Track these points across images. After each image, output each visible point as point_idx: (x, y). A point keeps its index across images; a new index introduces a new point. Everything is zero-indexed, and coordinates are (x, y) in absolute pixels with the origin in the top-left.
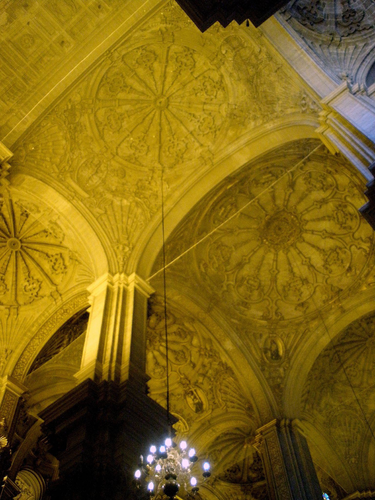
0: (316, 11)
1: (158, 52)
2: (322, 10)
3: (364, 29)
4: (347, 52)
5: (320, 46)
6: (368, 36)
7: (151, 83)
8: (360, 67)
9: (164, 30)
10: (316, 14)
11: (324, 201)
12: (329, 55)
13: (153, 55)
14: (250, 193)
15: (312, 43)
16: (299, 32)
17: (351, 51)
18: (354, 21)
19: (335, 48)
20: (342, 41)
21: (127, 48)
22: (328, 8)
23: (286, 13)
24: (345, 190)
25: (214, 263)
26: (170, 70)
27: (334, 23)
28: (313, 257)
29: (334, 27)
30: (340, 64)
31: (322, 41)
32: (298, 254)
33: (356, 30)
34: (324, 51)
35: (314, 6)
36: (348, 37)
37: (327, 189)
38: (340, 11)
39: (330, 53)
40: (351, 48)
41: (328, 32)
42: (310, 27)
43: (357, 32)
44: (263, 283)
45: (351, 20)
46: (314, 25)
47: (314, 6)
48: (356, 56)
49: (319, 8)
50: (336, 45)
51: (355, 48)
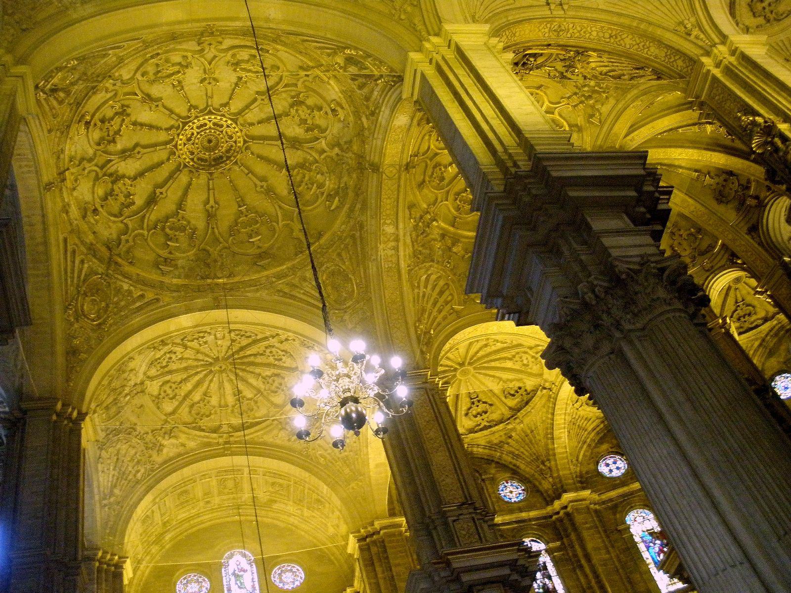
1: (187, 409)
7: (214, 386)
9: (167, 437)
11: (125, 154)
13: (193, 412)
14: (209, 223)
21: (207, 437)
24: (89, 172)
25: (321, 186)
26: (189, 386)
28: (196, 81)
32: (212, 97)
37: (111, 175)
44: (290, 100)
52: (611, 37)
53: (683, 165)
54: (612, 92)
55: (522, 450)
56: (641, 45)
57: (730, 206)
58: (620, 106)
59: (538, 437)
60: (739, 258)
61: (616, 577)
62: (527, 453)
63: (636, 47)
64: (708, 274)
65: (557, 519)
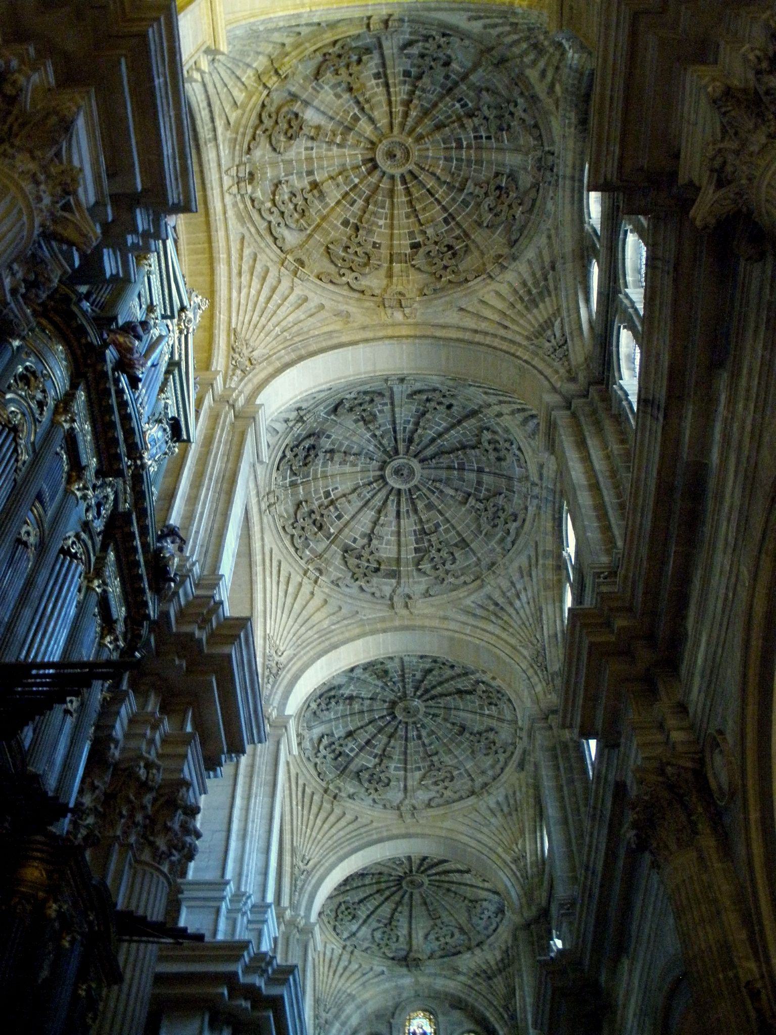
0: (339, 78)
2: (333, 87)
3: (254, 138)
4: (239, 84)
5: (283, 45)
6: (239, 137)
8: (206, 91)
10: (337, 73)
12: (259, 50)
15: (299, 34)
16: (332, 25)
17: (236, 93)
18: (277, 128)
19: (260, 70)
20: (261, 88)
22: (328, 99)
23: (382, 26)
27: (298, 93)
29: (293, 89)
30: (234, 59)
31: (287, 55)
33: (261, 122)
34: (271, 46)
35: (349, 79)
36: (260, 102)
38: (310, 116)
39: (258, 53)
40: (240, 96)
41: (294, 74)
42: (325, 50)
43: (257, 122)
45: (284, 125)
46: (321, 59)
47: (349, 79)
48: (223, 96)
49: (339, 84)
50: (264, 73)
51: (235, 103)
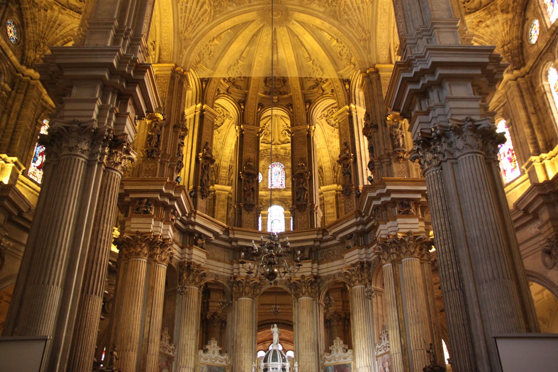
52: (384, 9)
53: (279, 54)
54: (329, 9)
55: (42, 23)
56: (383, 27)
57: (265, 87)
58: (321, 15)
59: (58, 31)
60: (244, 106)
61: (24, 142)
62: (41, 29)
63: (382, 25)
64: (226, 93)
65: (19, 77)
